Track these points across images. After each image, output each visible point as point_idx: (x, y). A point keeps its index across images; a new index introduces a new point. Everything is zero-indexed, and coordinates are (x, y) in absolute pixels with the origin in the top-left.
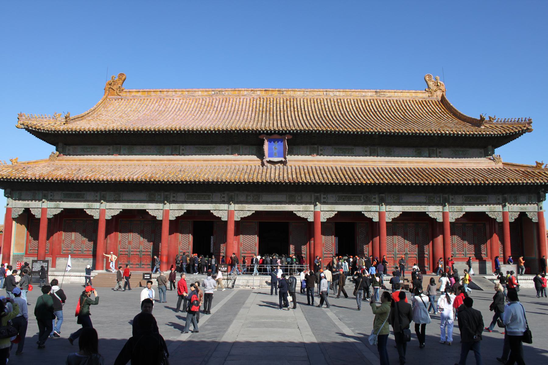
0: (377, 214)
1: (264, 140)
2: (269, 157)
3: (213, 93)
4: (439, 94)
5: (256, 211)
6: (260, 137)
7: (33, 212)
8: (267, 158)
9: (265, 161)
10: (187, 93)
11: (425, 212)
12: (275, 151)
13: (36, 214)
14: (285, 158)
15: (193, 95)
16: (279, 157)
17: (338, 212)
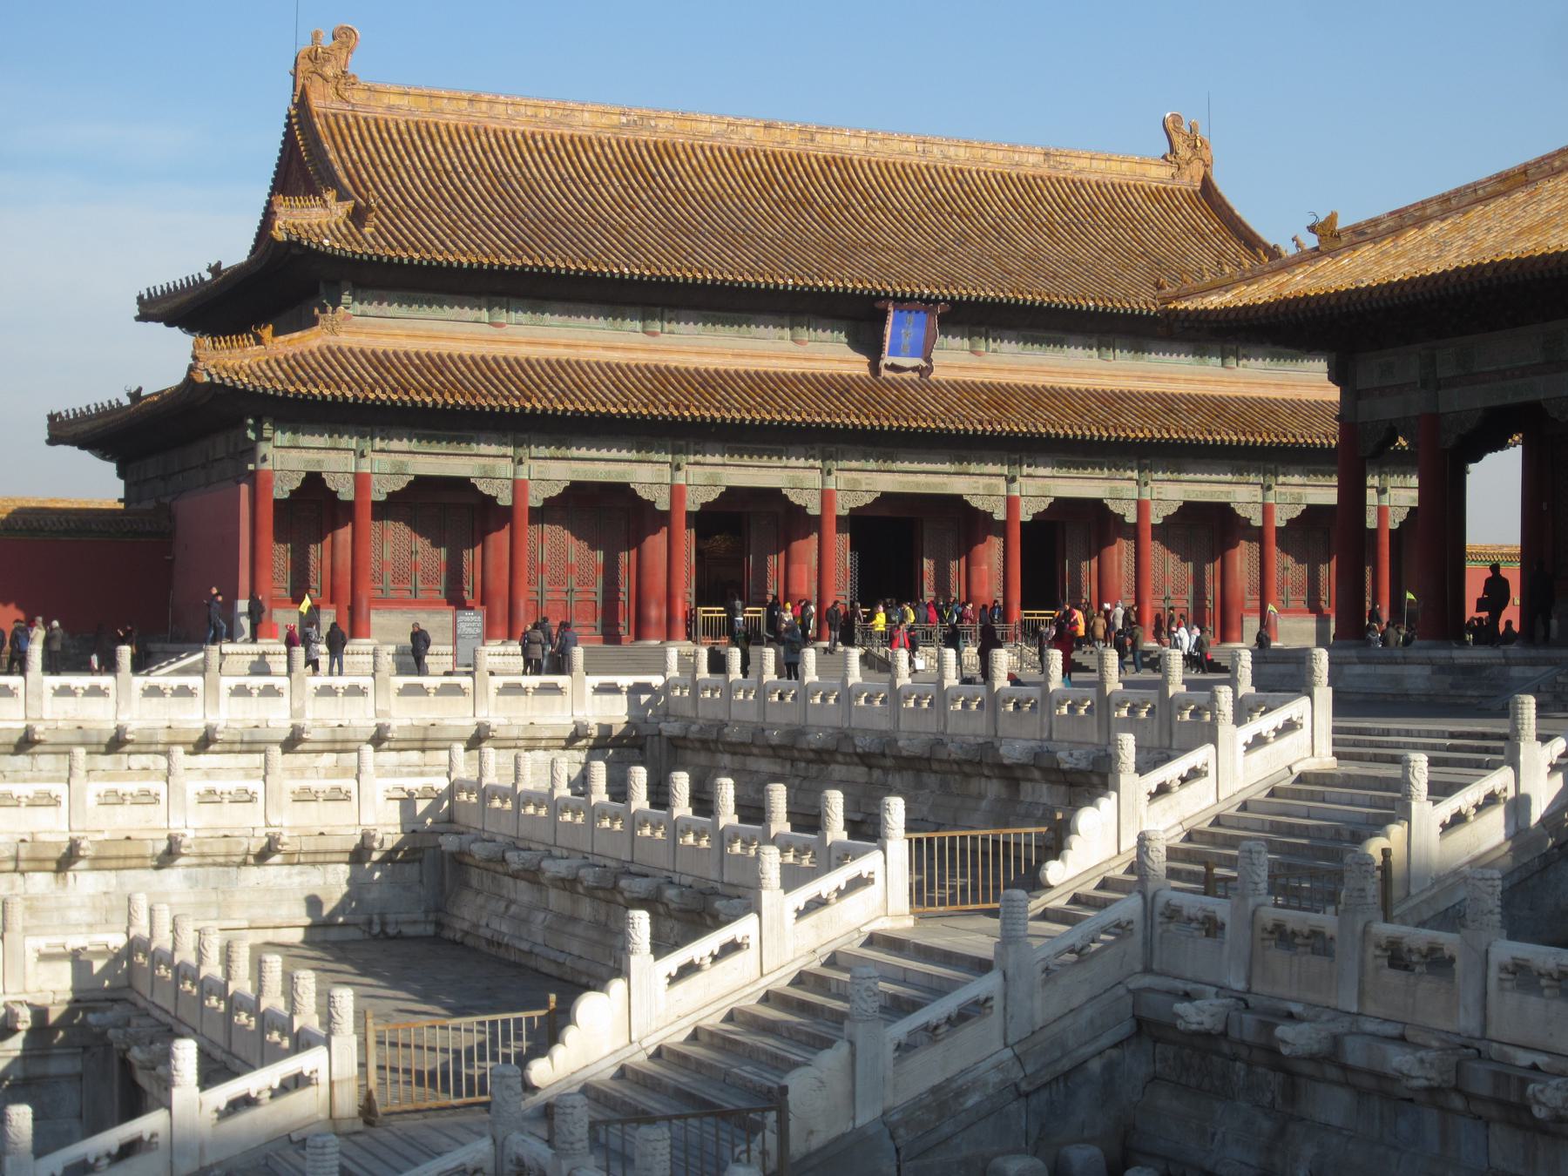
0: (1134, 505)
1: (885, 313)
2: (890, 354)
3: (624, 120)
4: (1197, 170)
5: (883, 494)
6: (880, 305)
7: (330, 485)
8: (887, 359)
9: (882, 363)
10: (548, 112)
11: (1228, 504)
12: (906, 341)
13: (341, 490)
14: (928, 360)
15: (567, 121)
16: (912, 356)
17: (1057, 499)
